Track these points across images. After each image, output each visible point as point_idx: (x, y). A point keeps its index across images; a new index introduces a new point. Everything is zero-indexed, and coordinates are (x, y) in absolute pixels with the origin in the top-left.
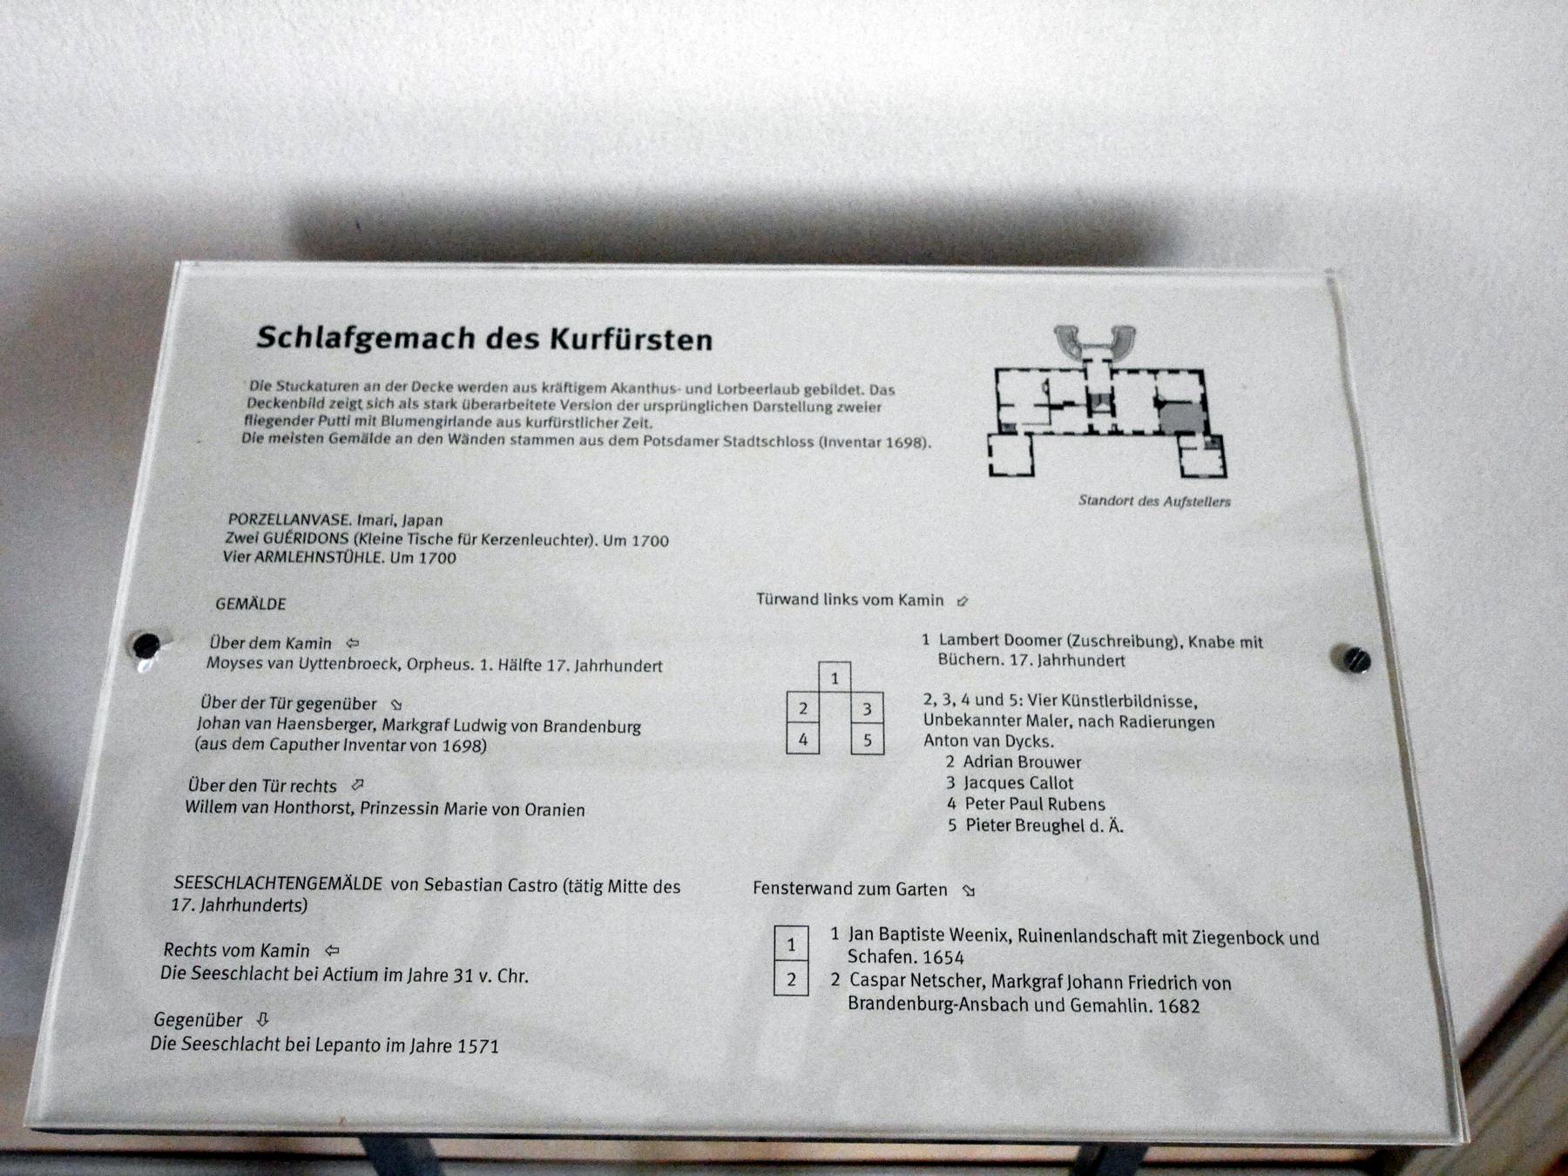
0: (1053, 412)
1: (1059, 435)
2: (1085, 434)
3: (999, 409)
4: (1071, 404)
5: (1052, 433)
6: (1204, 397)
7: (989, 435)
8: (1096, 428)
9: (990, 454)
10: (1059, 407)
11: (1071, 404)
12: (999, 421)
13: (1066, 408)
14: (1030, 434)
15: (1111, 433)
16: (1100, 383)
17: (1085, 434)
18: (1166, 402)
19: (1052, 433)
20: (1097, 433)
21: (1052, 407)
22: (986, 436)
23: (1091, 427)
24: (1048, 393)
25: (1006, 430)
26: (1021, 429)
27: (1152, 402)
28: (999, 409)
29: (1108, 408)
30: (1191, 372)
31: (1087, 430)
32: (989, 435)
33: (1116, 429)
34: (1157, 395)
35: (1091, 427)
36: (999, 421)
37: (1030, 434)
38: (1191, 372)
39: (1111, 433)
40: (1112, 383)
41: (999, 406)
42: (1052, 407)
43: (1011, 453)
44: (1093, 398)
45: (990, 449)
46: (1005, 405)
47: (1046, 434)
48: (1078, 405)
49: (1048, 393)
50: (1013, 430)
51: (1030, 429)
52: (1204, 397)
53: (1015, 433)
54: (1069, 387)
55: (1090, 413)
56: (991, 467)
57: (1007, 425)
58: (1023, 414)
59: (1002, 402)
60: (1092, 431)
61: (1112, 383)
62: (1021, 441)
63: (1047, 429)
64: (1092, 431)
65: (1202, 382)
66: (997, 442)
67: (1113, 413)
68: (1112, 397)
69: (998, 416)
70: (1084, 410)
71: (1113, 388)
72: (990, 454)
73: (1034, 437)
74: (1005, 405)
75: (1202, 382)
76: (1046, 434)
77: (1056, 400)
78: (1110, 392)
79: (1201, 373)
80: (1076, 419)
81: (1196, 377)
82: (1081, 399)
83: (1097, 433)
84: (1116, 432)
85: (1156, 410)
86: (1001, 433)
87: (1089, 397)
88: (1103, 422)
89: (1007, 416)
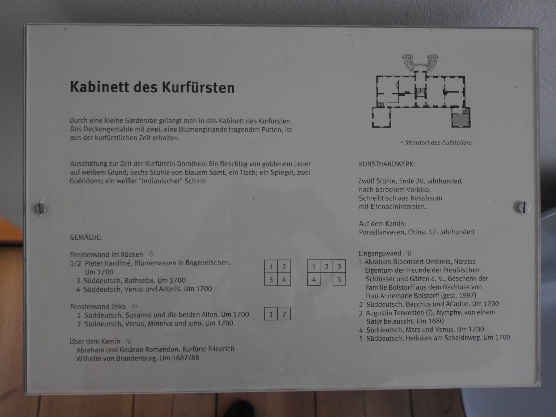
0: (400, 96)
1: (402, 108)
2: (413, 107)
3: (377, 96)
4: (408, 93)
5: (399, 107)
6: (464, 89)
7: (373, 108)
8: (417, 105)
9: (373, 117)
10: (402, 94)
11: (408, 93)
12: (377, 101)
13: (405, 95)
14: (389, 108)
15: (424, 107)
16: (421, 84)
17: (413, 107)
18: (448, 92)
19: (399, 107)
20: (418, 107)
21: (400, 94)
22: (372, 109)
23: (416, 103)
24: (398, 87)
25: (380, 106)
26: (386, 105)
27: (442, 91)
28: (377, 96)
29: (424, 95)
30: (460, 77)
31: (414, 106)
32: (373, 108)
33: (426, 105)
34: (445, 88)
35: (416, 103)
36: (377, 101)
37: (389, 108)
38: (460, 77)
39: (424, 107)
40: (426, 83)
41: (377, 94)
42: (400, 94)
43: (381, 116)
44: (417, 90)
45: (373, 114)
46: (379, 94)
47: (396, 107)
48: (411, 94)
49: (398, 87)
50: (383, 106)
51: (390, 105)
52: (464, 89)
53: (383, 107)
54: (407, 85)
55: (416, 97)
56: (373, 123)
57: (380, 103)
58: (388, 98)
59: (378, 93)
60: (416, 106)
61: (426, 83)
62: (386, 110)
63: (397, 105)
64: (416, 106)
65: (464, 82)
66: (376, 111)
67: (426, 98)
68: (426, 89)
69: (377, 99)
70: (414, 95)
71: (426, 85)
72: (373, 117)
73: (391, 108)
74: (379, 94)
75: (464, 82)
76: (396, 107)
77: (402, 91)
78: (425, 87)
79: (463, 78)
80: (409, 100)
81: (462, 79)
82: (412, 91)
83: (418, 107)
84: (426, 106)
85: (444, 95)
86: (378, 107)
87: (416, 89)
88: (421, 102)
89: (381, 99)
